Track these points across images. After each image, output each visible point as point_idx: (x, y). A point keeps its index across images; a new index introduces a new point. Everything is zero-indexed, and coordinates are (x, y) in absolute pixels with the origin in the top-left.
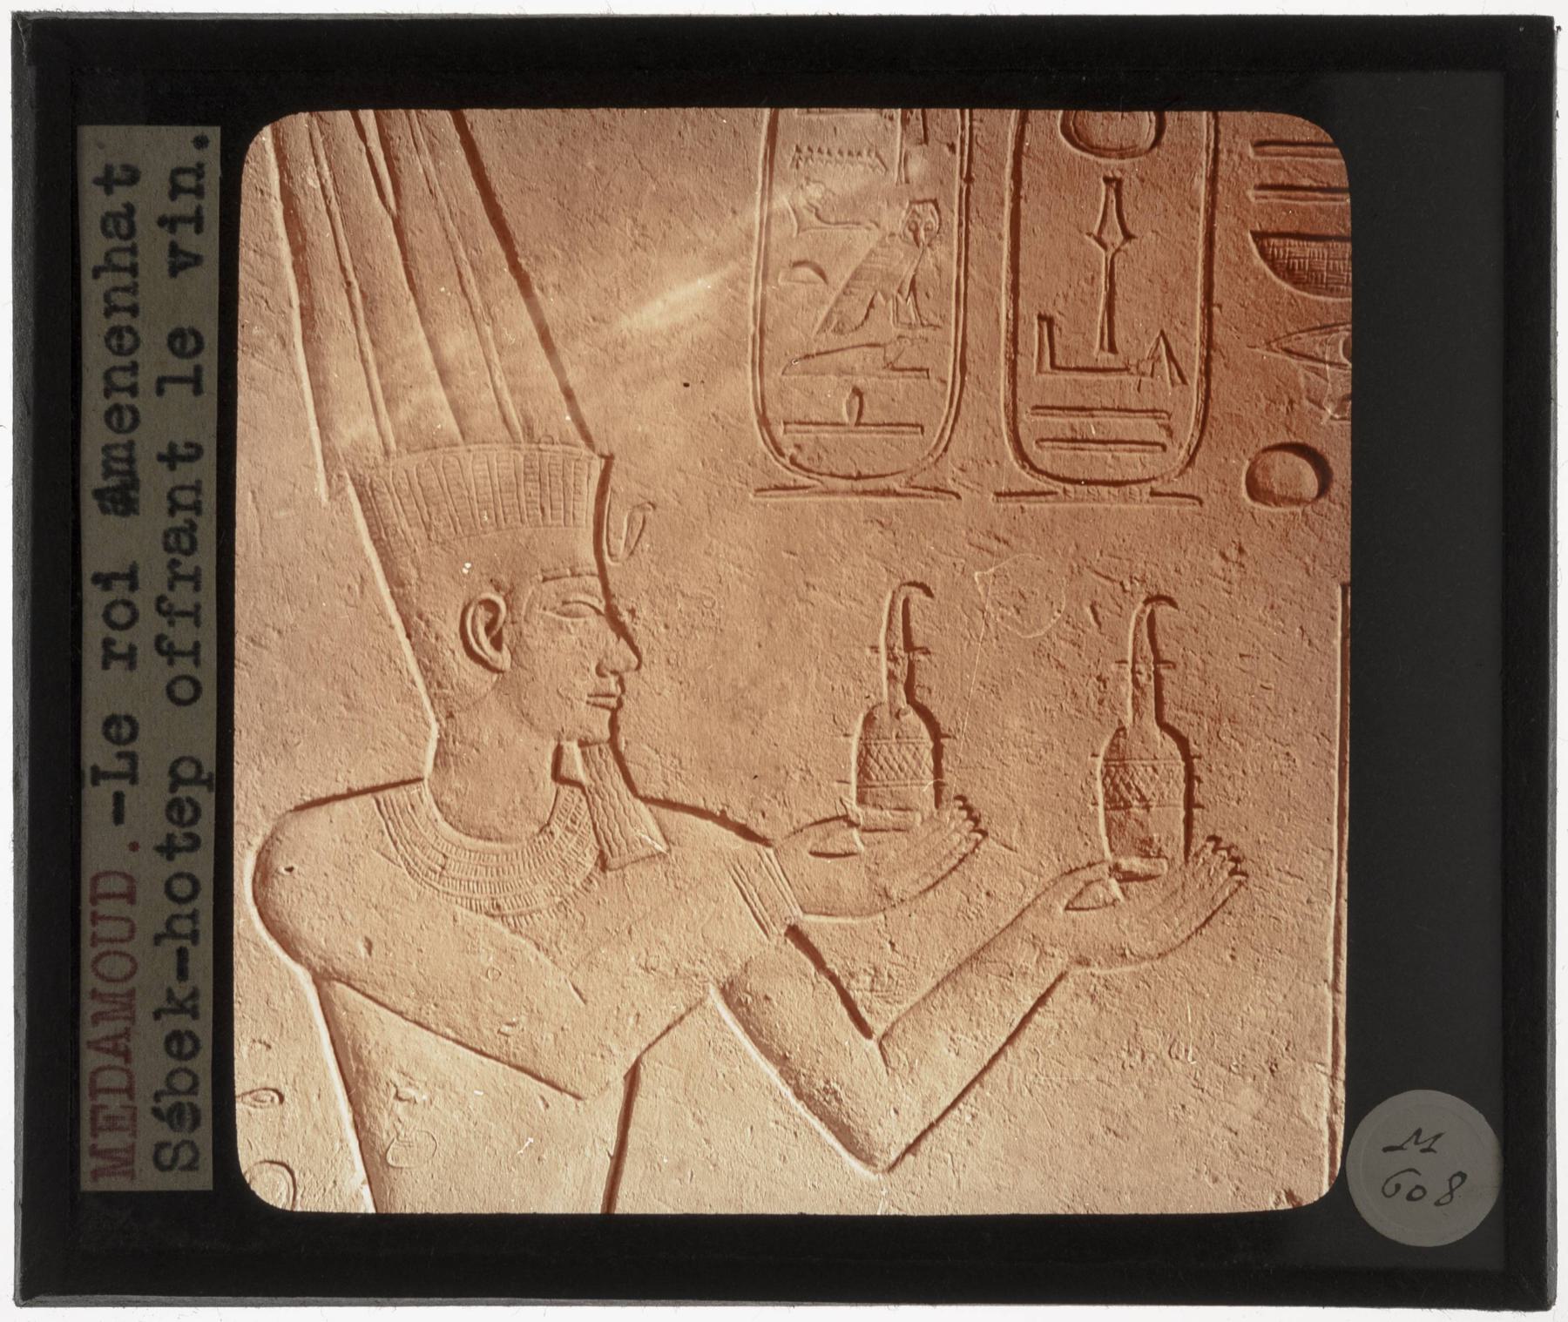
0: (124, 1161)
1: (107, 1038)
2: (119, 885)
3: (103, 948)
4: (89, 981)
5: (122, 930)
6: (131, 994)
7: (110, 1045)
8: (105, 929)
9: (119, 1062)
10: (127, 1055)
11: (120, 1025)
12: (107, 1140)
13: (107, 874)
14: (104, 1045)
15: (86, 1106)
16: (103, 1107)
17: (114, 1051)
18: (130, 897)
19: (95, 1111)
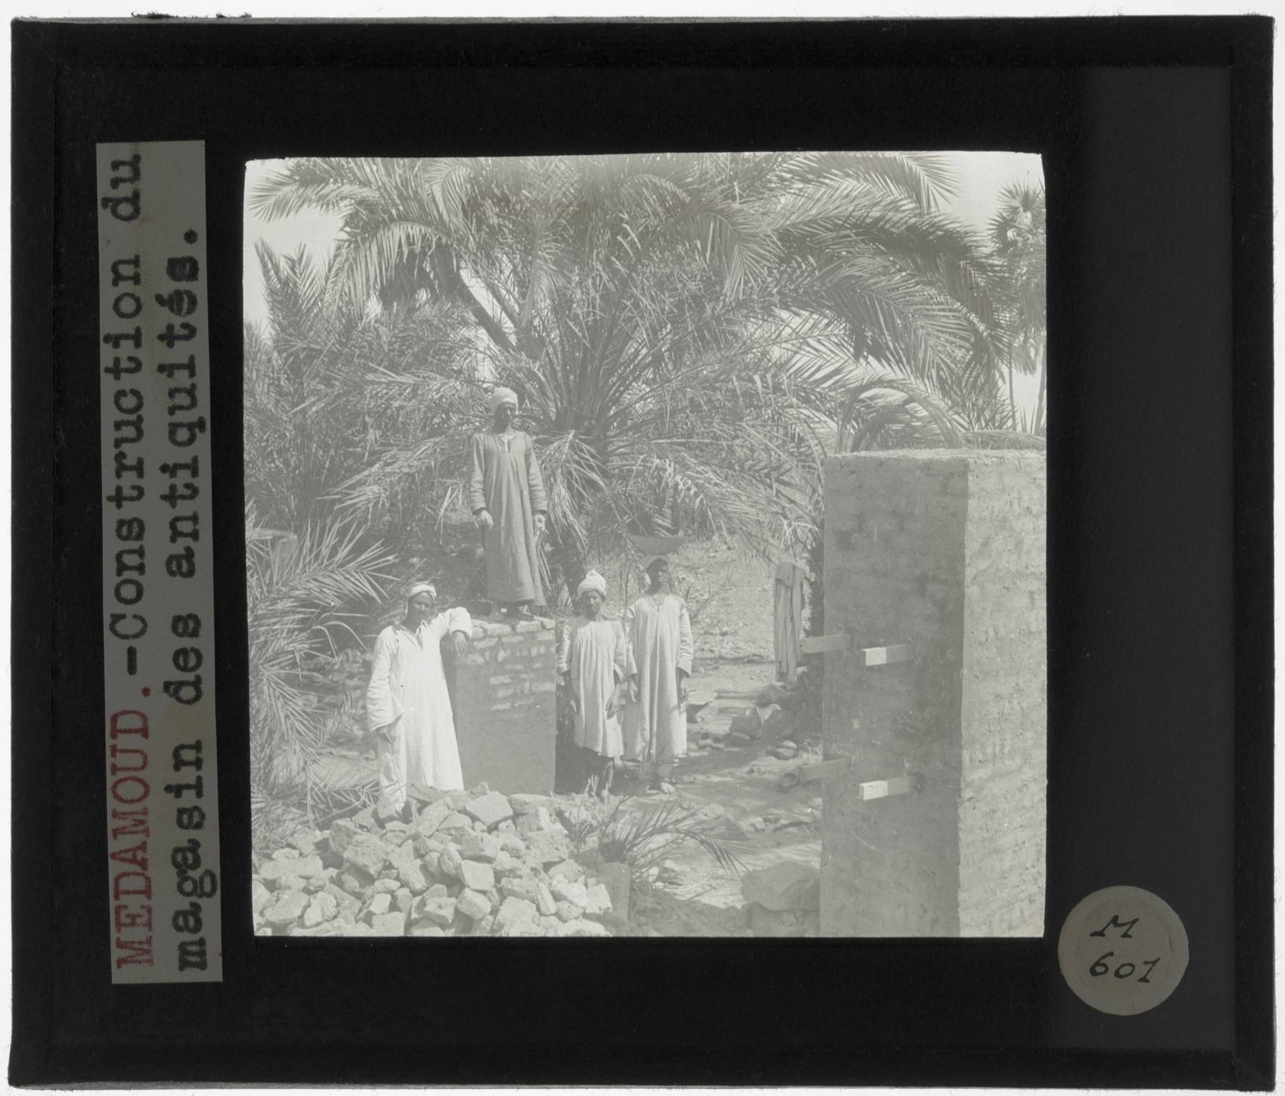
0: (144, 951)
1: (127, 851)
2: (136, 723)
3: (121, 775)
4: (111, 804)
5: (136, 760)
6: (145, 812)
7: (129, 855)
8: (122, 760)
9: (137, 869)
10: (143, 864)
11: (136, 840)
12: (127, 934)
13: (124, 713)
14: (123, 855)
15: (113, 904)
16: (125, 907)
17: (133, 861)
18: (144, 732)
19: (118, 909)
